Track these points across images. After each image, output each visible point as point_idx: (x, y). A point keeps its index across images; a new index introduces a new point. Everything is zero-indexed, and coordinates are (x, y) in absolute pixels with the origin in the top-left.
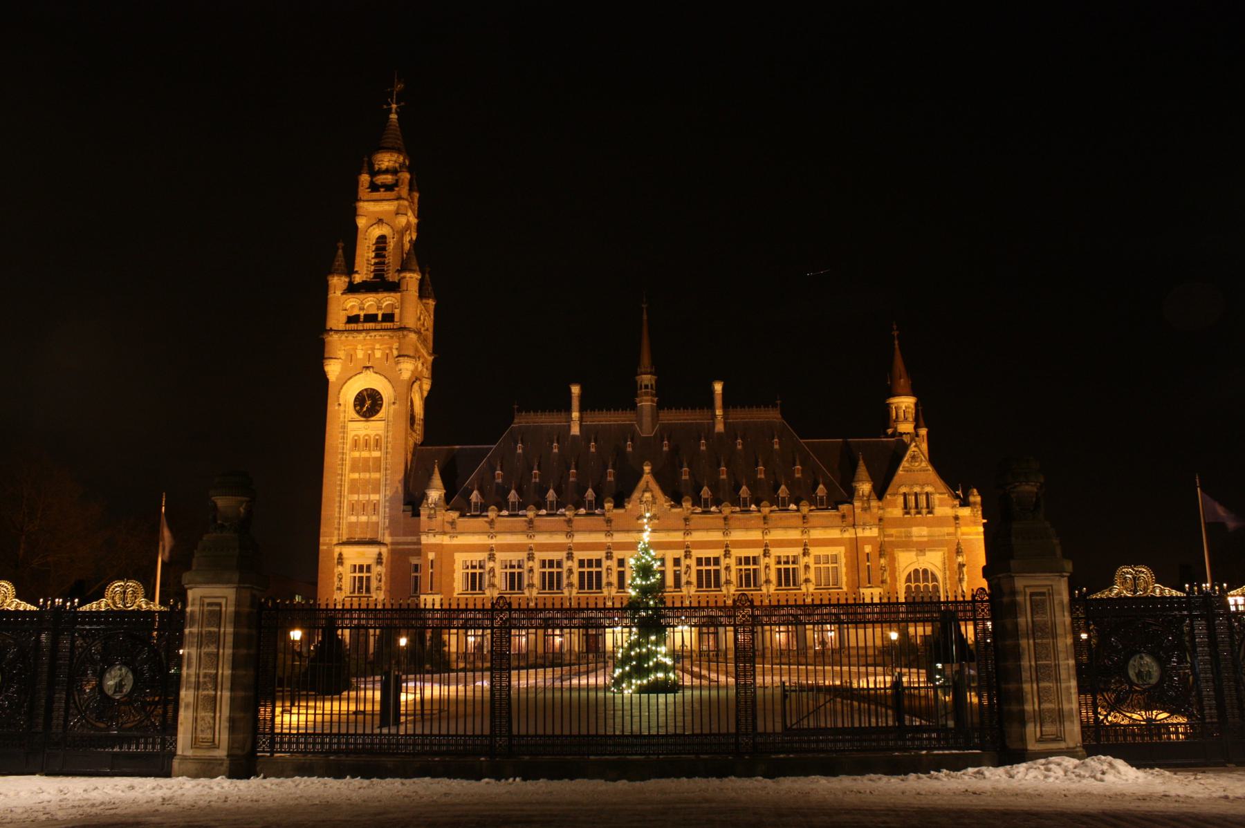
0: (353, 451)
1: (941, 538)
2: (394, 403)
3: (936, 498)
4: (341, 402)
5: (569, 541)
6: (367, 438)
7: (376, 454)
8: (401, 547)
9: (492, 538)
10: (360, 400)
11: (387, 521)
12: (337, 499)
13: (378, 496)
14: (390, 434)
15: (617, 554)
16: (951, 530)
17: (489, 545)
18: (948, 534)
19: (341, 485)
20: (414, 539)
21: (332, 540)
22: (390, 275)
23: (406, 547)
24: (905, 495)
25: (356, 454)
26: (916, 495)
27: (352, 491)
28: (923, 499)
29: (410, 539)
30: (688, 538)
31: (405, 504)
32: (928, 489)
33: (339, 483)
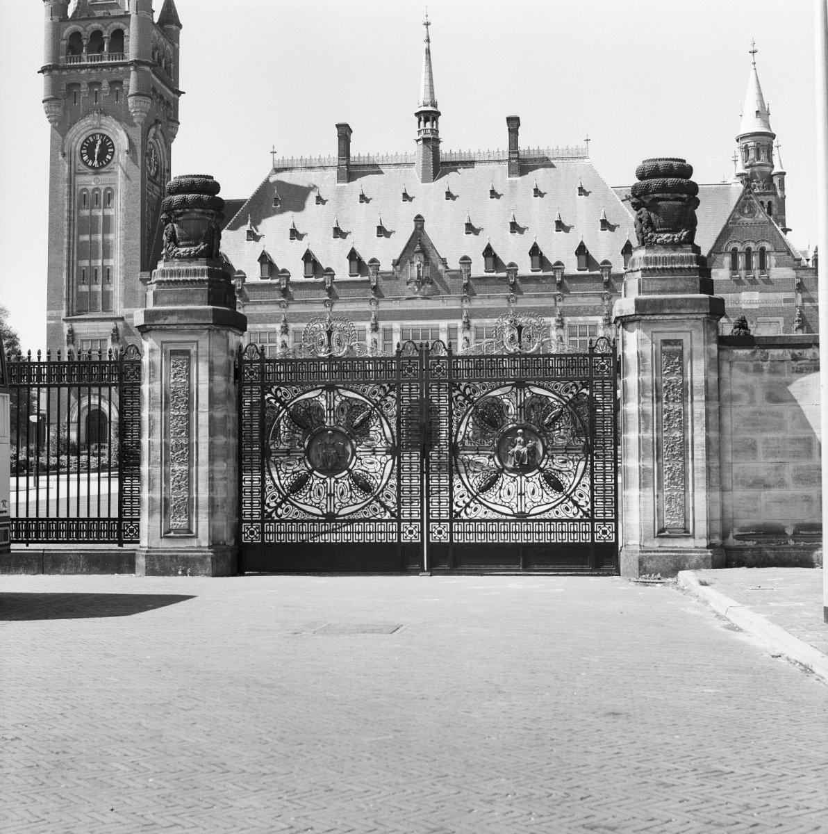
0: (80, 208)
1: (776, 305)
2: (127, 151)
3: (771, 260)
4: (66, 151)
5: (329, 309)
7: (108, 212)
10: (89, 147)
12: (65, 265)
15: (382, 324)
16: (790, 295)
18: (786, 301)
24: (734, 254)
26: (749, 249)
27: (79, 258)
28: (755, 260)
30: (466, 306)
31: (142, 270)
32: (768, 246)
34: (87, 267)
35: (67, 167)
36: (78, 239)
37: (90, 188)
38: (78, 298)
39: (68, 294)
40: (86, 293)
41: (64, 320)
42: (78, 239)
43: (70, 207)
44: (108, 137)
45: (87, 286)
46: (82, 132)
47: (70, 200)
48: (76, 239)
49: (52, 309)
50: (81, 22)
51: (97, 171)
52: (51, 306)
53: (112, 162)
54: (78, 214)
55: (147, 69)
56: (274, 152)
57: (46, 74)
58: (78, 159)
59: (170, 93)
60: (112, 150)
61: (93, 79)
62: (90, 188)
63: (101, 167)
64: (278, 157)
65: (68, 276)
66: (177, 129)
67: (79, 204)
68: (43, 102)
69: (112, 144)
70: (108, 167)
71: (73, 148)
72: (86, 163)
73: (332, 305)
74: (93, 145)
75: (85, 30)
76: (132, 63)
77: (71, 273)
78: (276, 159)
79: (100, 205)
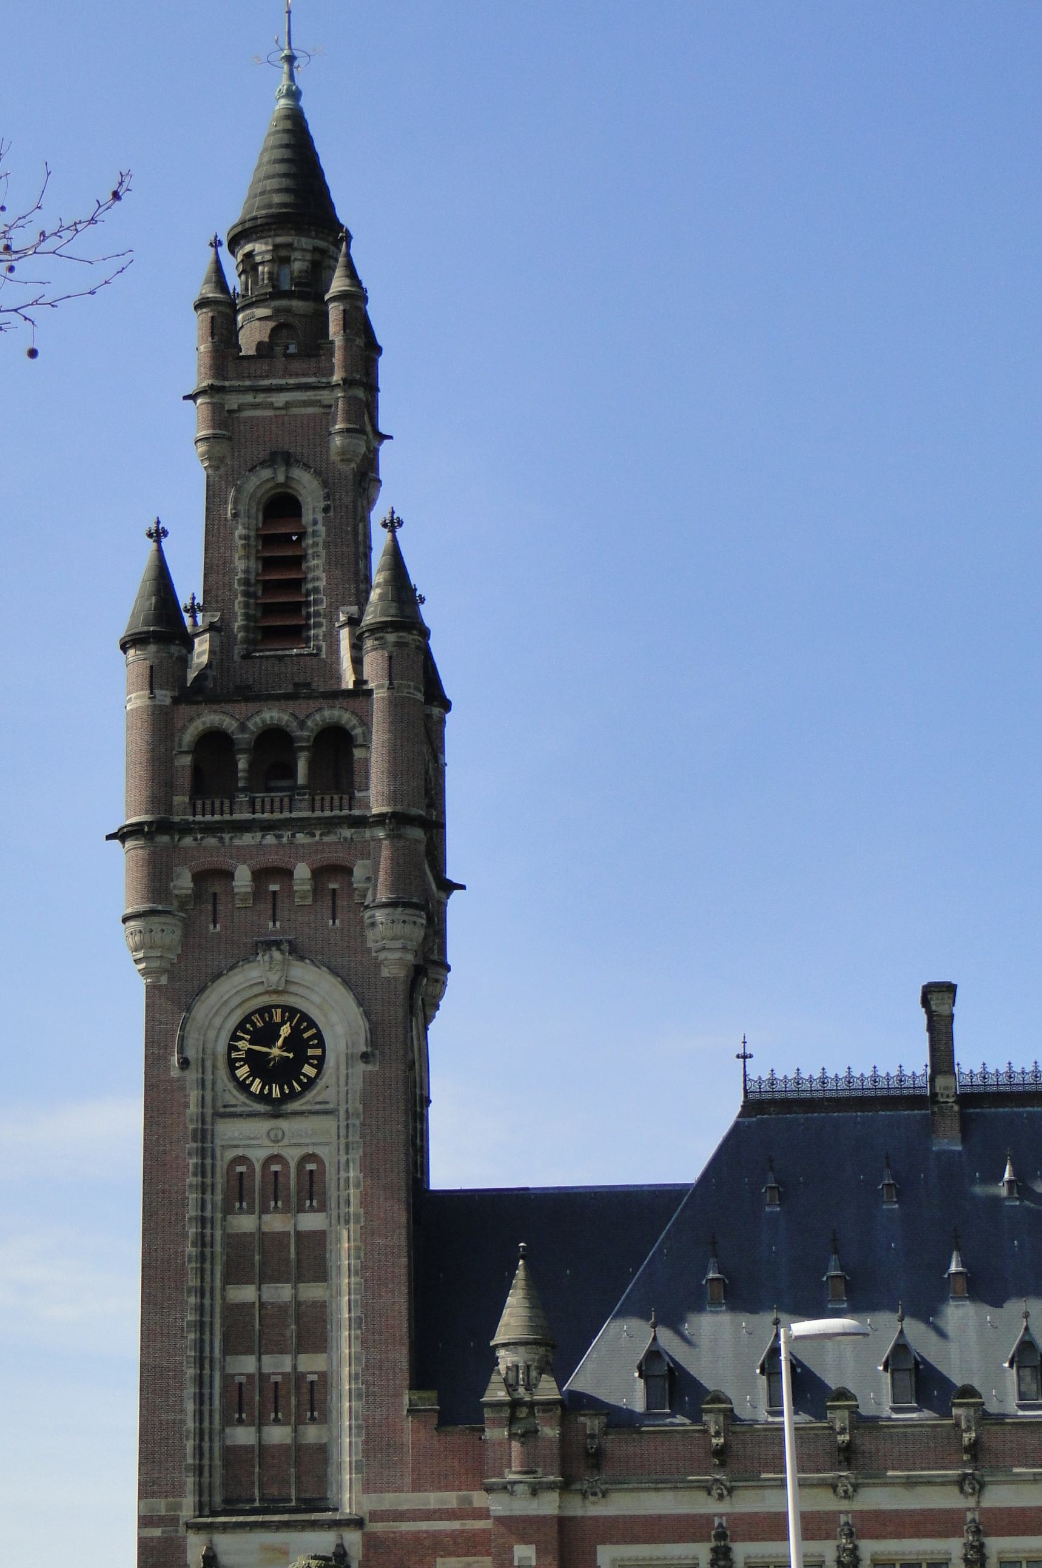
0: (228, 1210)
2: (365, 1057)
4: (191, 1053)
5: (971, 1502)
6: (276, 1168)
7: (311, 1222)
8: (406, 1527)
9: (721, 1497)
11: (360, 1440)
12: (191, 1372)
13: (325, 1355)
14: (356, 1155)
17: (708, 1519)
19: (202, 1324)
20: (450, 1499)
21: (178, 1507)
22: (321, 631)
23: (424, 1526)
25: (245, 1223)
29: (433, 1499)
31: (412, 1388)
33: (191, 1317)
34: (250, 1376)
35: (194, 1095)
36: (223, 1298)
37: (258, 1156)
38: (226, 1465)
39: (199, 1451)
40: (247, 1449)
41: (189, 1526)
42: (223, 1298)
43: (203, 1208)
44: (305, 1017)
45: (253, 1429)
46: (237, 1000)
47: (203, 1188)
48: (218, 1292)
49: (153, 1495)
50: (228, 707)
51: (276, 1109)
52: (146, 1490)
53: (321, 1083)
54: (224, 1228)
55: (416, 833)
56: (745, 1057)
57: (129, 844)
58: (223, 1072)
59: (434, 886)
60: (318, 1052)
61: (273, 859)
62: (258, 1156)
63: (285, 1098)
64: (758, 1070)
65: (200, 1399)
66: (444, 984)
67: (223, 1200)
68: (125, 920)
69: (319, 1035)
70: (310, 1096)
71: (209, 1046)
72: (243, 1087)
73: (980, 1487)
74: (268, 1035)
75: (243, 727)
76: (381, 819)
77: (206, 1391)
78: (753, 1075)
79: (287, 1202)
